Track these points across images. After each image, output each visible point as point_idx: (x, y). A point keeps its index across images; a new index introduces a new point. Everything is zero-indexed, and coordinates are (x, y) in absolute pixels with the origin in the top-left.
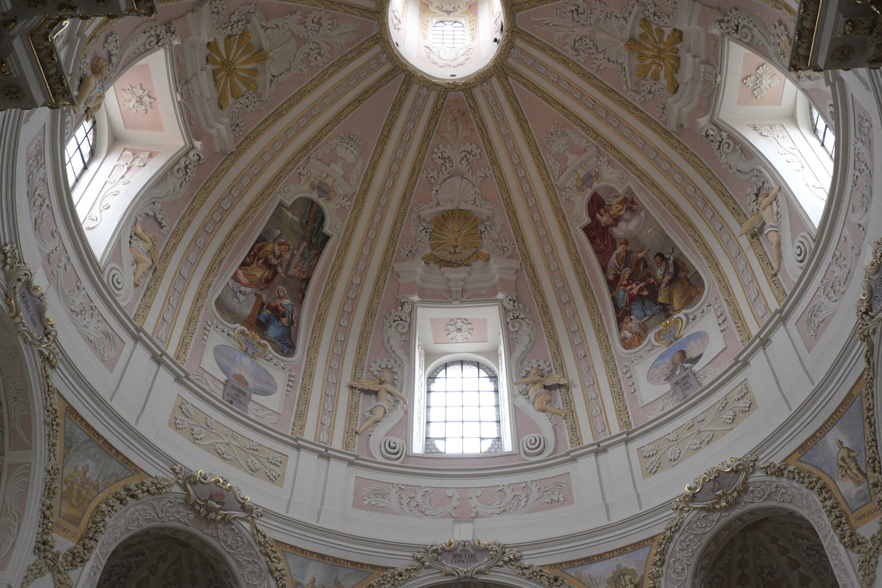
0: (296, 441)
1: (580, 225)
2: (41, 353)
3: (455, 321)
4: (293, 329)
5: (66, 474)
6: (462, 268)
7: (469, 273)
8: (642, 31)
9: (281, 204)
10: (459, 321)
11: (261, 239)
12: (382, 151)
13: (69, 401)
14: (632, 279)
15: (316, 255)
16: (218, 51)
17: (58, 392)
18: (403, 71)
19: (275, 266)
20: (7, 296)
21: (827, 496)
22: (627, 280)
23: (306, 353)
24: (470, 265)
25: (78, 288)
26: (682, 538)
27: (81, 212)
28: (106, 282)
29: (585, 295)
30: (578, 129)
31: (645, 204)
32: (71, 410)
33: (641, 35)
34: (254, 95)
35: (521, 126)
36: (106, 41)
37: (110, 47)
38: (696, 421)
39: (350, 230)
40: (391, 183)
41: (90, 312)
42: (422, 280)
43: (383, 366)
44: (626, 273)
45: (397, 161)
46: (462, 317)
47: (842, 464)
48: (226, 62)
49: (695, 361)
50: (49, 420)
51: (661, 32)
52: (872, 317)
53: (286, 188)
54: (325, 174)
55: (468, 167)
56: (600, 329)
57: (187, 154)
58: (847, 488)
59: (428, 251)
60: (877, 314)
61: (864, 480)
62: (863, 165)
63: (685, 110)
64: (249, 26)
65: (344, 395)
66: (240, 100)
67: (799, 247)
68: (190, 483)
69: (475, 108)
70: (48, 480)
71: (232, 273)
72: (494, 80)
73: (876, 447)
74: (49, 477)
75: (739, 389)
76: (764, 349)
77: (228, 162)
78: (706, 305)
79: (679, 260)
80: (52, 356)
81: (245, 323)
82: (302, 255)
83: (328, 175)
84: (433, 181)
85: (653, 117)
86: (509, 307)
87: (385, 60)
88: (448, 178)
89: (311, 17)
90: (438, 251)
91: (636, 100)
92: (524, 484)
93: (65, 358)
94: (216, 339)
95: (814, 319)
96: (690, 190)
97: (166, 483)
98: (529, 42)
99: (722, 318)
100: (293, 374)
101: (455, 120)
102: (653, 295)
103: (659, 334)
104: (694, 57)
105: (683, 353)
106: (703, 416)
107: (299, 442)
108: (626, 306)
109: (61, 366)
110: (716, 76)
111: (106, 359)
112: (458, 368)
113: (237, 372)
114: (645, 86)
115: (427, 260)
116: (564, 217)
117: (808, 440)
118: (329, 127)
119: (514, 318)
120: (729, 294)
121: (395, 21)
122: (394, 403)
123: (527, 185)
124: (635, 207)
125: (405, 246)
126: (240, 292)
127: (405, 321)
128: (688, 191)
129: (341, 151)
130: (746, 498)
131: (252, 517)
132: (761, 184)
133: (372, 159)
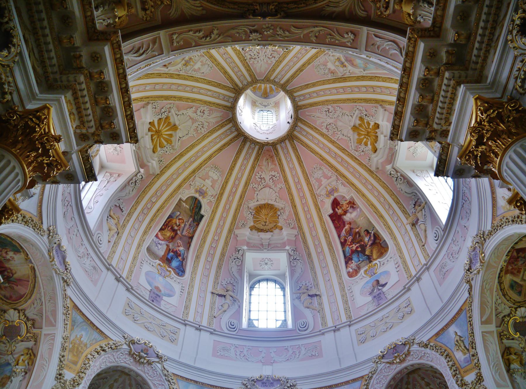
0: (185, 321)
1: (328, 214)
2: (63, 278)
4: (184, 262)
5: (72, 339)
8: (360, 122)
9: (180, 199)
11: (170, 217)
12: (231, 174)
14: (353, 242)
16: (154, 126)
17: (70, 298)
19: (176, 230)
20: (49, 251)
21: (449, 360)
23: (190, 275)
26: (377, 377)
27: (85, 203)
28: (95, 240)
29: (329, 249)
30: (327, 166)
32: (76, 307)
33: (359, 124)
34: (170, 146)
35: (300, 164)
38: (384, 317)
39: (214, 212)
40: (235, 190)
41: (87, 256)
43: (228, 282)
44: (350, 238)
45: (238, 179)
46: (268, 258)
47: (457, 344)
49: (383, 286)
50: (65, 312)
51: (369, 124)
52: (471, 273)
54: (203, 185)
56: (336, 266)
57: (136, 175)
58: (459, 356)
59: (252, 224)
60: (474, 271)
61: (468, 352)
62: (467, 198)
63: (381, 161)
64: (170, 114)
67: (435, 233)
68: (132, 343)
69: (277, 154)
70: (63, 342)
73: (474, 336)
74: (63, 341)
75: (406, 302)
76: (418, 283)
77: (156, 179)
80: (68, 280)
81: (161, 259)
82: (190, 225)
85: (364, 163)
87: (234, 130)
89: (199, 109)
91: (356, 154)
92: (298, 346)
94: (146, 268)
95: (443, 270)
97: (120, 344)
100: (184, 286)
102: (363, 251)
103: (366, 271)
104: (385, 136)
105: (378, 281)
106: (387, 315)
107: (186, 322)
108: (350, 255)
109: (72, 285)
110: (395, 146)
115: (252, 228)
117: (440, 331)
118: (206, 162)
120: (401, 253)
121: (240, 112)
122: (233, 302)
123: (302, 193)
124: (355, 206)
126: (159, 243)
128: (381, 200)
129: (211, 174)
130: (409, 358)
133: (226, 178)
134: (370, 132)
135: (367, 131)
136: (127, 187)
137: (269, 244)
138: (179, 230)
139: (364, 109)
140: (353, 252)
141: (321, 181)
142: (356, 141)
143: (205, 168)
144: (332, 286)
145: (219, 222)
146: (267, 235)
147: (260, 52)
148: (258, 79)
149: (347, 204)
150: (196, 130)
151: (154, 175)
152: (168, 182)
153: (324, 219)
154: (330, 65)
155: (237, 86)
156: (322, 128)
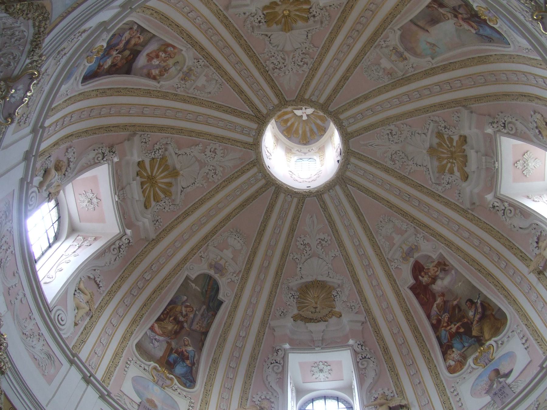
1: (408, 285)
4: (194, 369)
7: (327, 326)
9: (187, 278)
10: (321, 363)
11: (172, 302)
12: (260, 240)
13: (12, 401)
14: (450, 321)
16: (145, 170)
18: (273, 184)
19: (182, 322)
22: (447, 322)
25: (30, 318)
28: (52, 316)
30: (400, 216)
31: (455, 265)
33: (437, 144)
34: (170, 200)
35: (359, 218)
36: (67, 152)
37: (70, 155)
39: (238, 297)
40: (267, 264)
41: (38, 337)
44: (445, 317)
46: (323, 360)
48: (150, 177)
51: (451, 140)
53: (192, 266)
54: (219, 257)
55: (323, 250)
56: (429, 361)
59: (296, 312)
63: (476, 191)
64: (167, 153)
66: (159, 203)
71: (149, 326)
72: (338, 188)
78: (510, 331)
79: (484, 302)
81: (159, 361)
82: (202, 315)
83: (221, 258)
84: (298, 261)
85: (453, 201)
86: (358, 350)
88: (309, 258)
89: (209, 148)
90: (303, 311)
91: (439, 190)
93: (13, 367)
94: (134, 371)
96: (487, 249)
98: (360, 159)
99: (525, 338)
103: (476, 359)
104: (477, 152)
105: (497, 371)
108: (448, 342)
110: (494, 163)
111: (46, 374)
112: (322, 402)
113: (149, 397)
115: (295, 318)
116: (395, 281)
119: (363, 358)
121: (268, 154)
124: (447, 268)
125: (278, 309)
126: (155, 339)
127: (280, 363)
132: (539, 234)
135: (451, 151)
136: (106, 254)
137: (323, 340)
139: (441, 119)
145: (246, 310)
146: (321, 326)
147: (287, 58)
148: (287, 99)
149: (435, 266)
153: (403, 294)
154: (385, 64)
155: (259, 112)
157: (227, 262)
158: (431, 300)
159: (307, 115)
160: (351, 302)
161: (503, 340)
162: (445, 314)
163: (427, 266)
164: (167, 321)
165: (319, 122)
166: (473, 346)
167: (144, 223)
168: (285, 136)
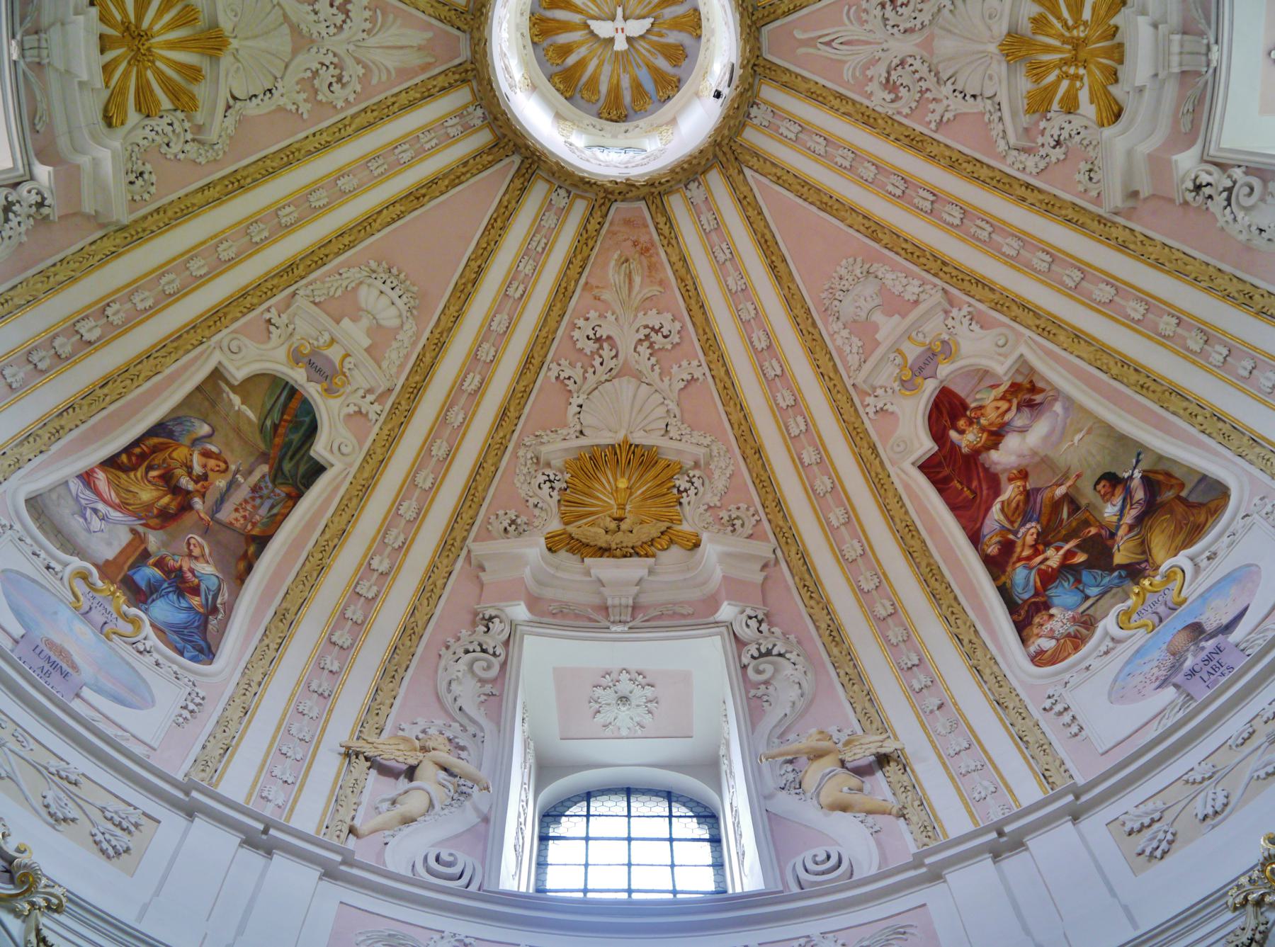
0: (187, 794)
3: (614, 676)
4: (213, 623)
6: (635, 559)
7: (651, 572)
10: (624, 676)
11: (159, 429)
14: (1043, 541)
15: (289, 496)
19: (188, 492)
22: (1034, 547)
24: (654, 556)
33: (1034, 20)
34: (187, 125)
35: (773, 267)
38: (1258, 724)
39: (376, 461)
42: (539, 583)
44: (1029, 532)
46: (633, 666)
48: (133, 28)
49: (1228, 628)
54: (327, 337)
55: (653, 360)
59: (555, 525)
63: (1145, 148)
65: (328, 764)
69: (670, 237)
77: (108, 245)
79: (1156, 472)
82: (255, 489)
83: (333, 341)
84: (571, 386)
85: (1067, 197)
87: (478, 122)
88: (607, 381)
91: (1025, 167)
101: (627, 260)
103: (1128, 613)
104: (1155, 26)
105: (1196, 630)
108: (1036, 594)
112: (617, 805)
113: (57, 639)
114: (1047, 133)
118: (346, 240)
119: (761, 655)
124: (1038, 398)
125: (501, 512)
126: (95, 511)
127: (494, 655)
129: (367, 296)
131: (33, 904)
134: (1085, 41)
137: (635, 608)
138: (203, 496)
140: (1048, 578)
141: (876, 328)
142: (1022, 104)
143: (342, 265)
144: (960, 721)
145: (397, 502)
146: (633, 569)
149: (1003, 398)
150: (309, 83)
151: (102, 226)
152: (164, 281)
153: (898, 485)
156: (868, 89)
157: (349, 355)
158: (985, 492)
159: (629, 40)
160: (732, 507)
161: (1213, 549)
162: (1028, 526)
163: (976, 400)
164: (139, 474)
165: (662, 63)
166: (1114, 591)
167: (96, 162)
168: (558, 90)
